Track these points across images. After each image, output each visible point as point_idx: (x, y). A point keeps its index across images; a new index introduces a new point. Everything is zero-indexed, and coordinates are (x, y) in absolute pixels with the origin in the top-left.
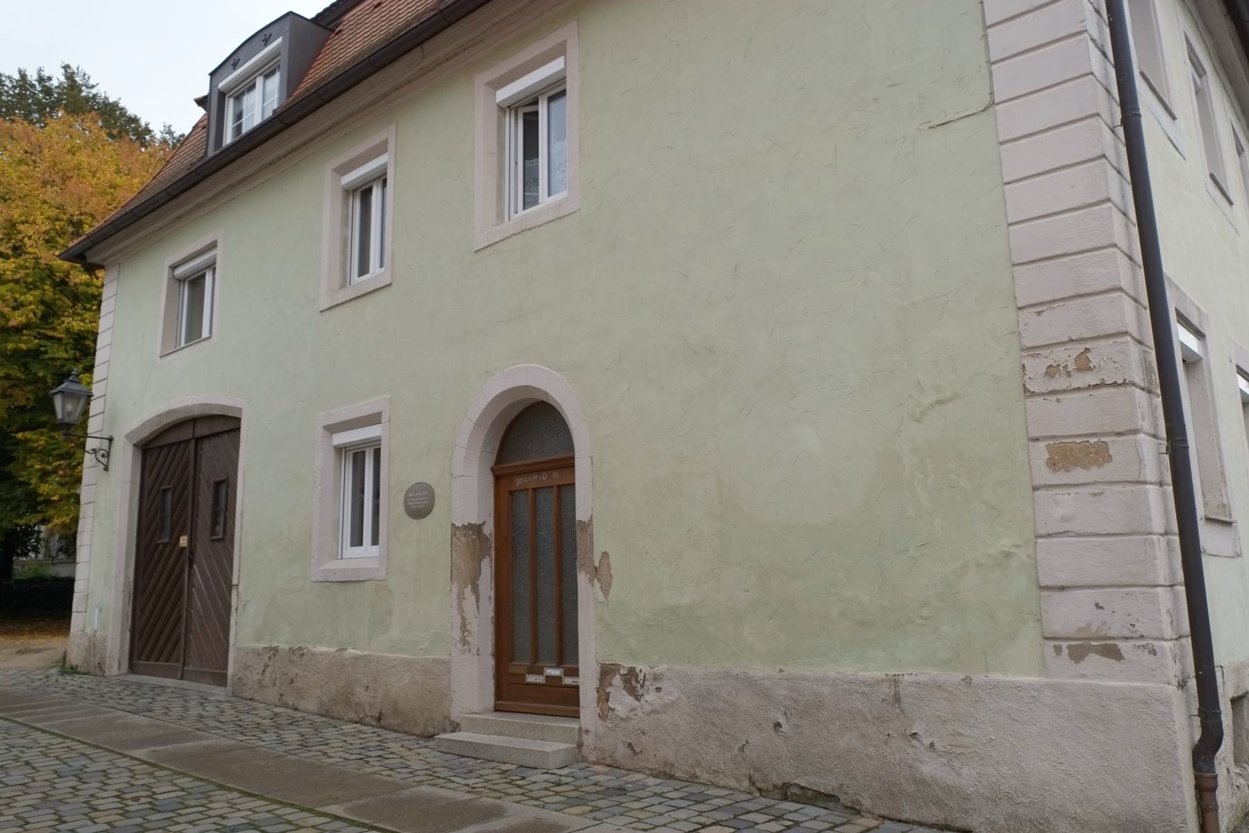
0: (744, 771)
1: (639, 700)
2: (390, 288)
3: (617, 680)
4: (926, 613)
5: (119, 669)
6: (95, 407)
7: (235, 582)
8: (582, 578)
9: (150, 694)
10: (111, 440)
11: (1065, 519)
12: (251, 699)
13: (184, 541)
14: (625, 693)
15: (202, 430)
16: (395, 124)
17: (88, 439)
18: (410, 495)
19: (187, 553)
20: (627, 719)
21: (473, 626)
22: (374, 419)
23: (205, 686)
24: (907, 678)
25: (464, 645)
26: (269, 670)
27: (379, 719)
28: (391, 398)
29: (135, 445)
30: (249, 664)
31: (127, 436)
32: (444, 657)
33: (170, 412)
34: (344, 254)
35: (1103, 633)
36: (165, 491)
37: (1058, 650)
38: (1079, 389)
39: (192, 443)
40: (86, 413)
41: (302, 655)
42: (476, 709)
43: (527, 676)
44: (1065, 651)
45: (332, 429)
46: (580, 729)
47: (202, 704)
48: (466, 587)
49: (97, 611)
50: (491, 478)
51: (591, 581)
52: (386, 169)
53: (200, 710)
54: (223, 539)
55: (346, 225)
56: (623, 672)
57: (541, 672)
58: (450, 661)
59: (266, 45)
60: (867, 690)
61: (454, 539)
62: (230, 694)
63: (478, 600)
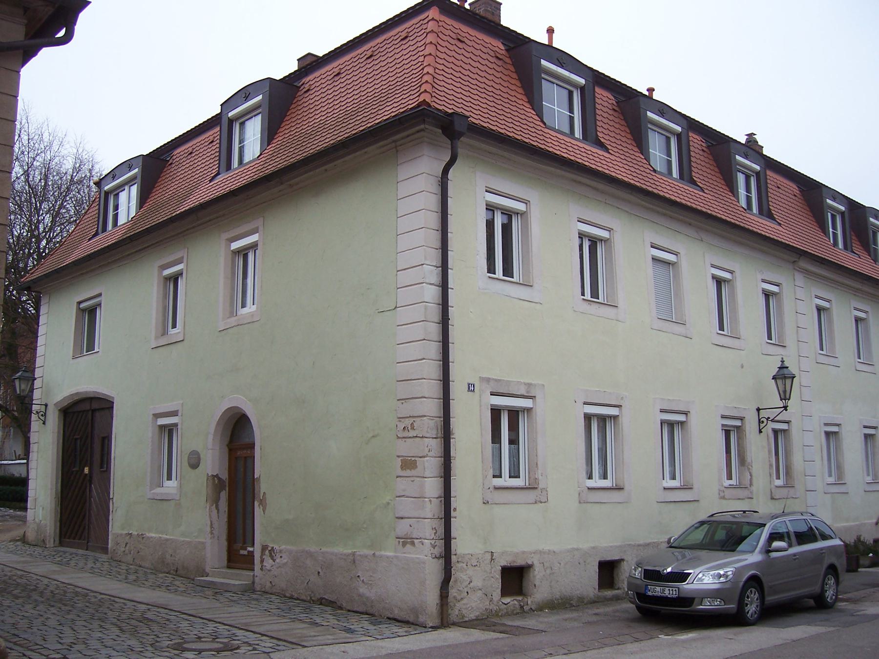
0: (308, 593)
1: (274, 562)
2: (183, 342)
3: (267, 552)
4: (365, 526)
5: (54, 543)
6: (37, 384)
7: (111, 497)
8: (256, 504)
9: (70, 557)
10: (46, 405)
11: (404, 490)
12: (120, 561)
13: (86, 470)
14: (269, 558)
15: (95, 405)
16: (187, 249)
17: (33, 405)
18: (191, 456)
19: (88, 478)
20: (269, 571)
21: (216, 525)
22: (174, 414)
23: (98, 554)
24: (358, 553)
25: (211, 534)
26: (128, 545)
27: (177, 571)
28: (182, 403)
29: (59, 410)
30: (119, 542)
31: (55, 404)
32: (203, 540)
33: (77, 394)
34: (164, 315)
35: (410, 537)
36: (76, 439)
37: (399, 542)
38: (410, 437)
39: (90, 412)
40: (32, 390)
41: (143, 538)
42: (217, 567)
43: (241, 551)
44: (401, 543)
45: (157, 416)
46: (254, 575)
47: (94, 562)
48: (212, 505)
49: (41, 508)
50: (227, 450)
51: (259, 505)
52: (183, 271)
53: (93, 565)
54: (106, 471)
55: (166, 298)
56: (269, 549)
57: (246, 550)
58: (205, 542)
59: (130, 171)
60: (345, 557)
61: (208, 481)
62: (110, 558)
63: (218, 513)
